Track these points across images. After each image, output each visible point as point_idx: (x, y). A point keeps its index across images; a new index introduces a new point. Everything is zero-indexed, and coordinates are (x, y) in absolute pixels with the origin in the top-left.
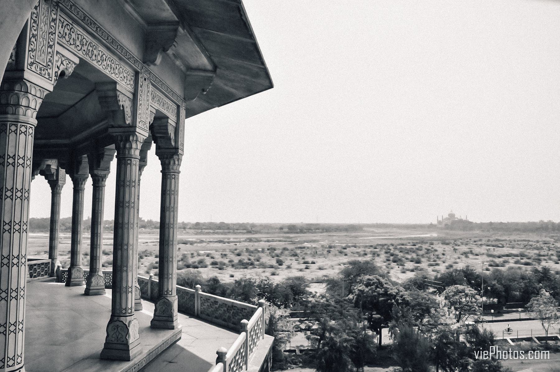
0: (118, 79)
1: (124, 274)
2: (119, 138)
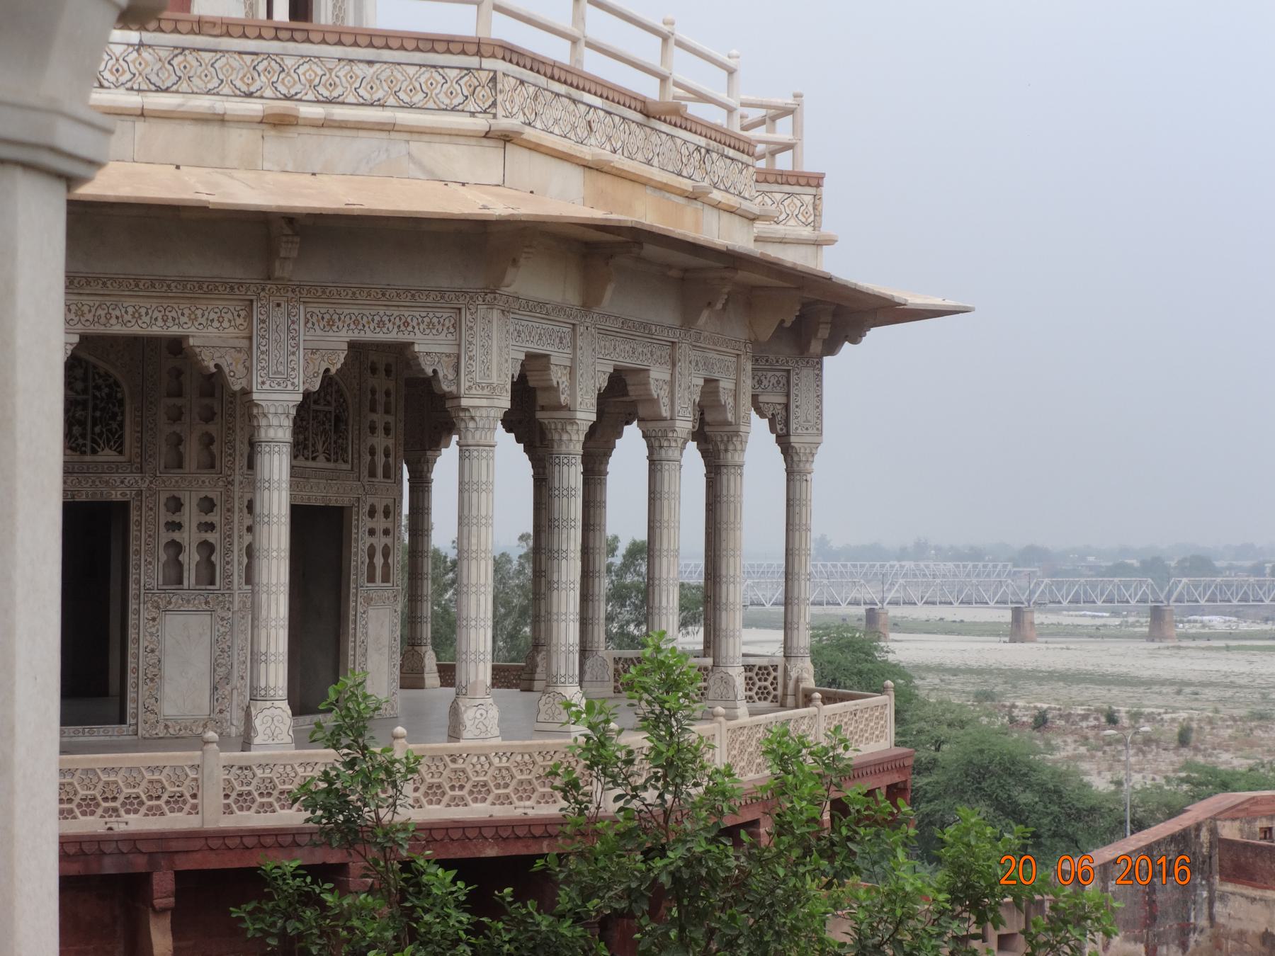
0: (193, 329)
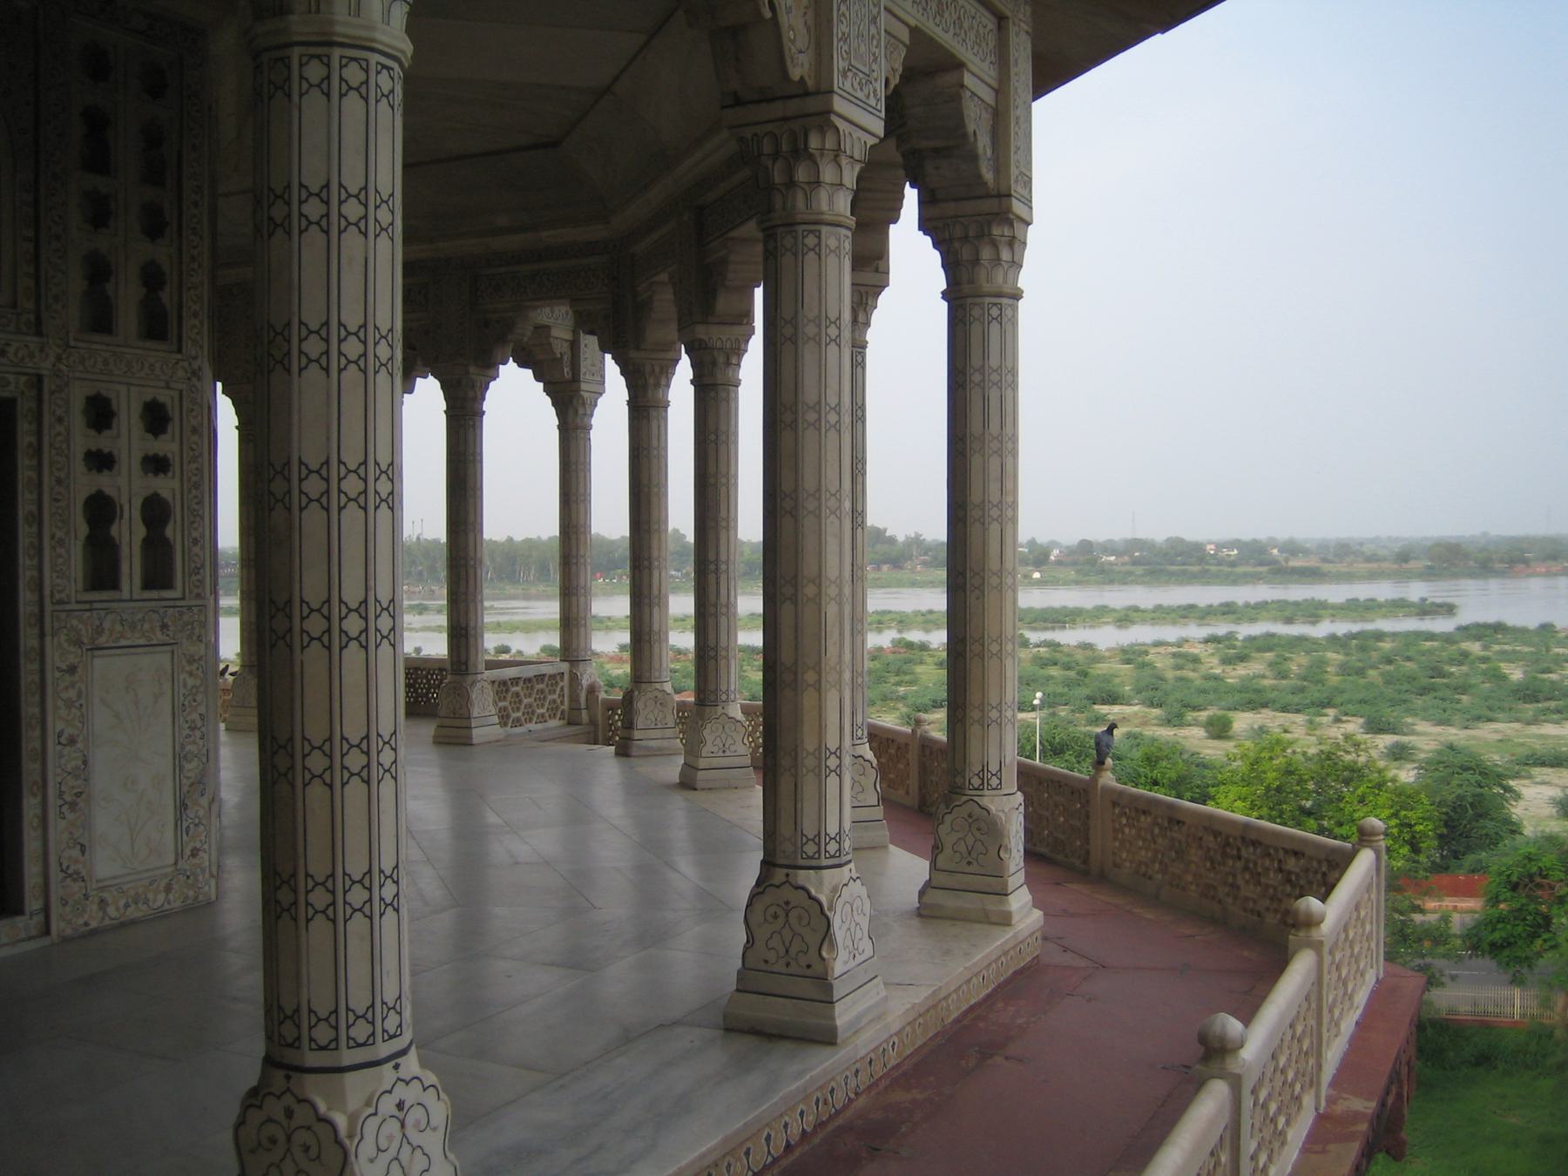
1: (808, 699)
2: (767, 148)
